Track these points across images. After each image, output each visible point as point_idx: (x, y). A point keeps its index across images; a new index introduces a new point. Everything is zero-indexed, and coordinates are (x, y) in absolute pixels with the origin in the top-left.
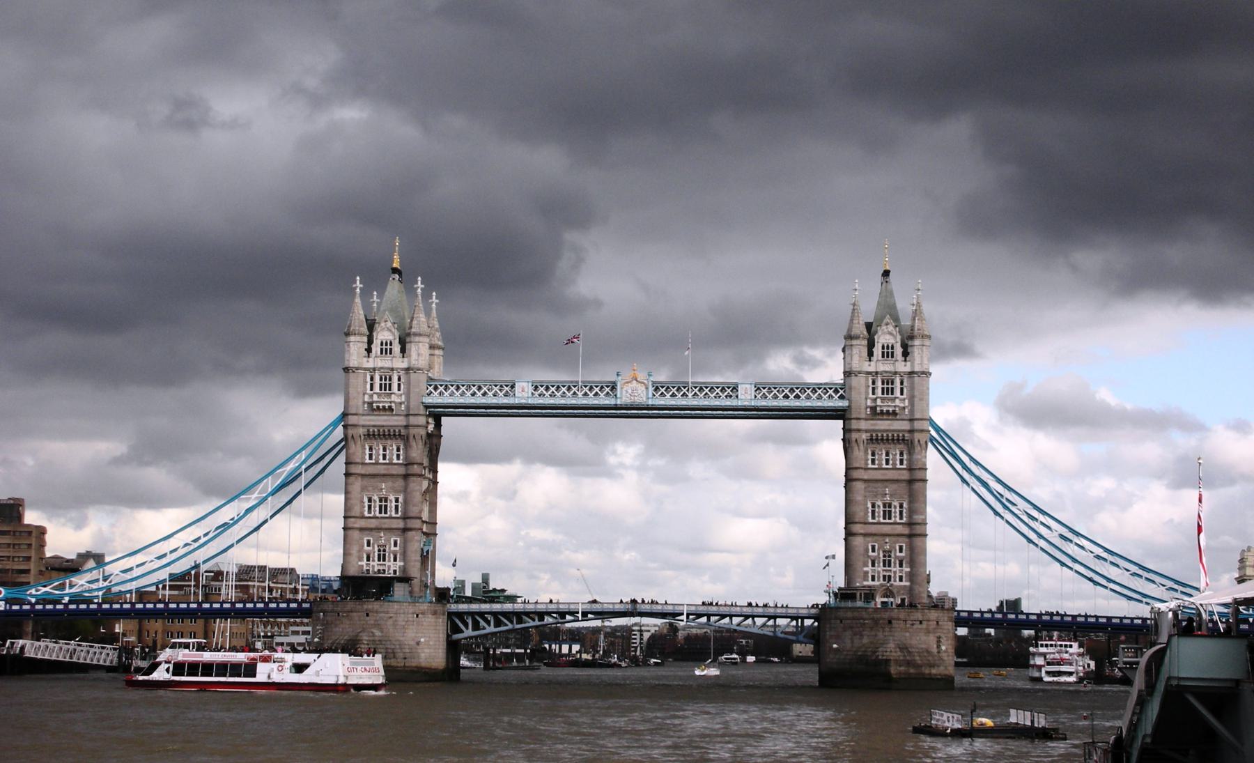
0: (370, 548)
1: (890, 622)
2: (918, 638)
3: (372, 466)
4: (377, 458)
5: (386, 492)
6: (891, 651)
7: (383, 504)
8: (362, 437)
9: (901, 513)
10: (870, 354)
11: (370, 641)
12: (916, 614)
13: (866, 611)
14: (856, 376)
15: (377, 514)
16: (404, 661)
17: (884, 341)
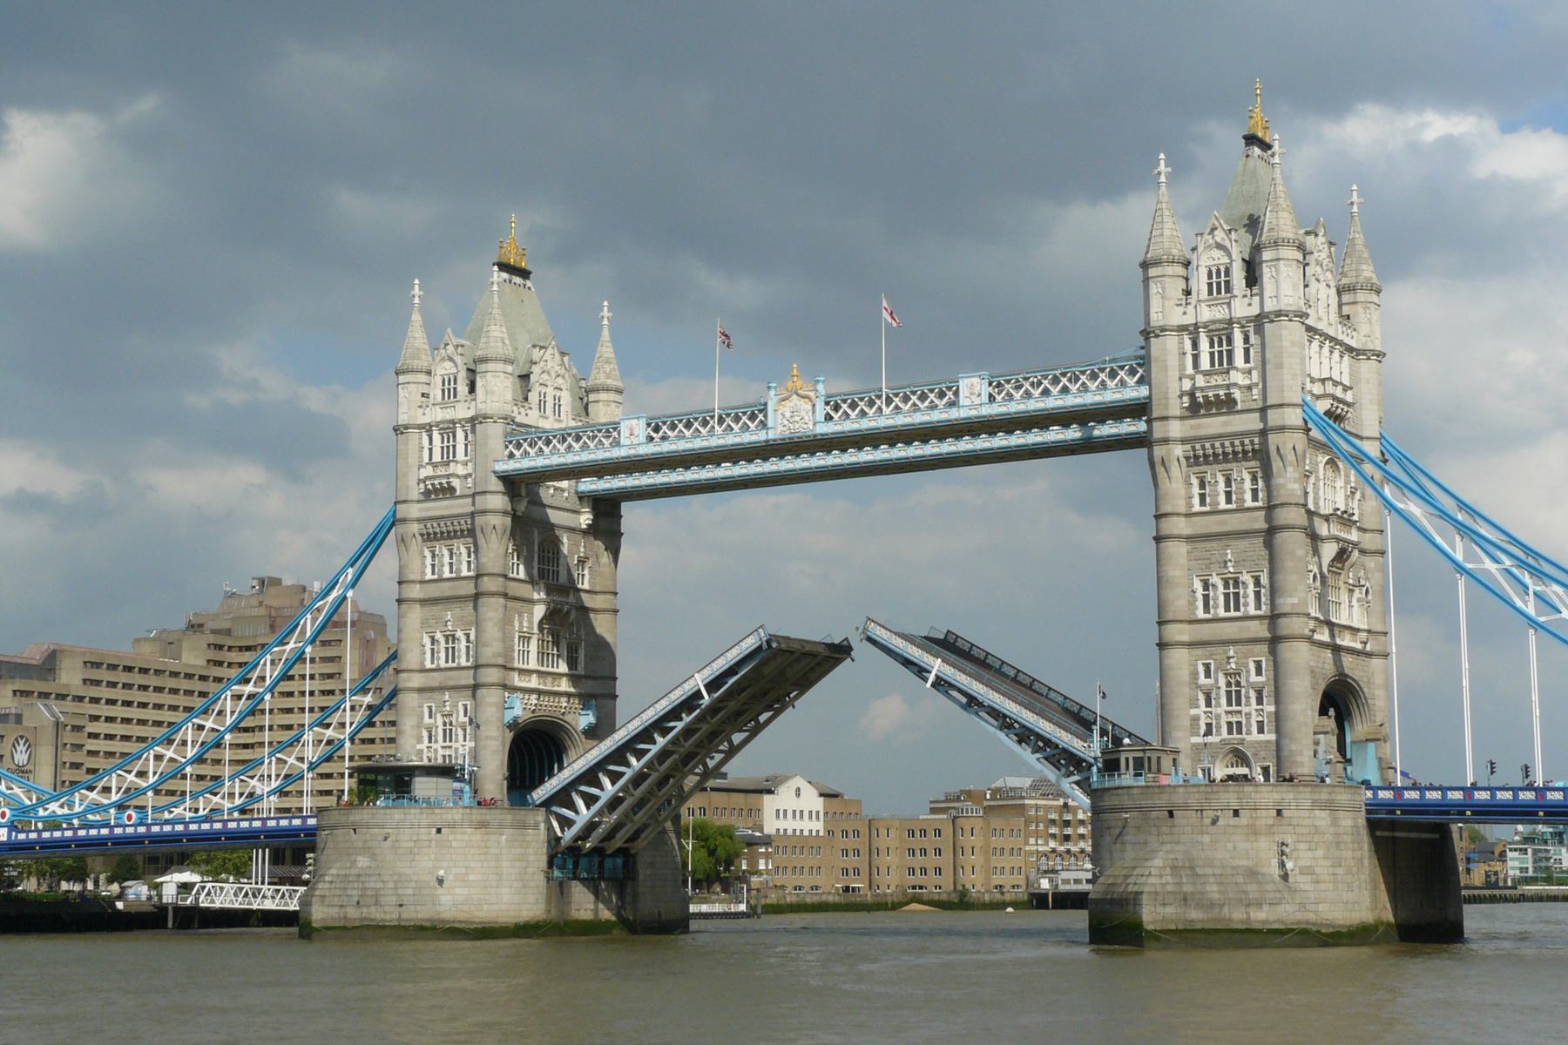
0: (432, 721)
1: (1171, 814)
2: (1230, 846)
3: (433, 585)
4: (441, 571)
5: (452, 626)
6: (1150, 875)
7: (451, 645)
8: (419, 538)
9: (1258, 594)
10: (1188, 293)
11: (338, 875)
12: (1222, 795)
13: (1128, 794)
14: (1157, 336)
15: (443, 664)
16: (399, 909)
17: (1211, 262)
